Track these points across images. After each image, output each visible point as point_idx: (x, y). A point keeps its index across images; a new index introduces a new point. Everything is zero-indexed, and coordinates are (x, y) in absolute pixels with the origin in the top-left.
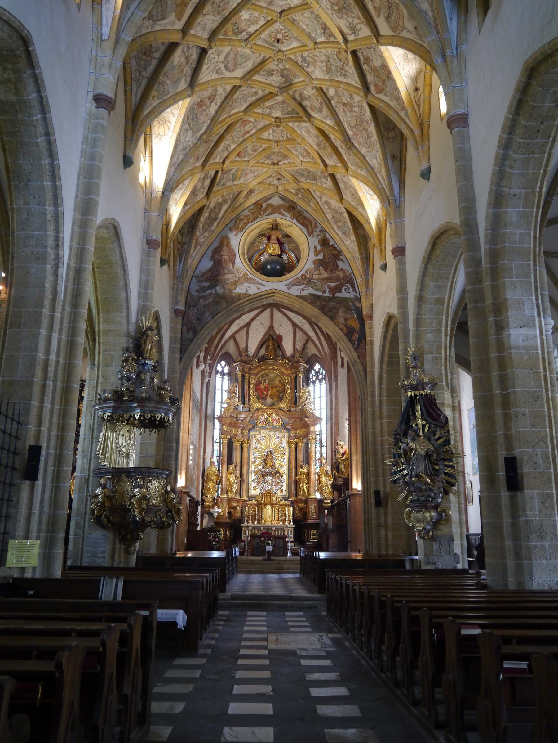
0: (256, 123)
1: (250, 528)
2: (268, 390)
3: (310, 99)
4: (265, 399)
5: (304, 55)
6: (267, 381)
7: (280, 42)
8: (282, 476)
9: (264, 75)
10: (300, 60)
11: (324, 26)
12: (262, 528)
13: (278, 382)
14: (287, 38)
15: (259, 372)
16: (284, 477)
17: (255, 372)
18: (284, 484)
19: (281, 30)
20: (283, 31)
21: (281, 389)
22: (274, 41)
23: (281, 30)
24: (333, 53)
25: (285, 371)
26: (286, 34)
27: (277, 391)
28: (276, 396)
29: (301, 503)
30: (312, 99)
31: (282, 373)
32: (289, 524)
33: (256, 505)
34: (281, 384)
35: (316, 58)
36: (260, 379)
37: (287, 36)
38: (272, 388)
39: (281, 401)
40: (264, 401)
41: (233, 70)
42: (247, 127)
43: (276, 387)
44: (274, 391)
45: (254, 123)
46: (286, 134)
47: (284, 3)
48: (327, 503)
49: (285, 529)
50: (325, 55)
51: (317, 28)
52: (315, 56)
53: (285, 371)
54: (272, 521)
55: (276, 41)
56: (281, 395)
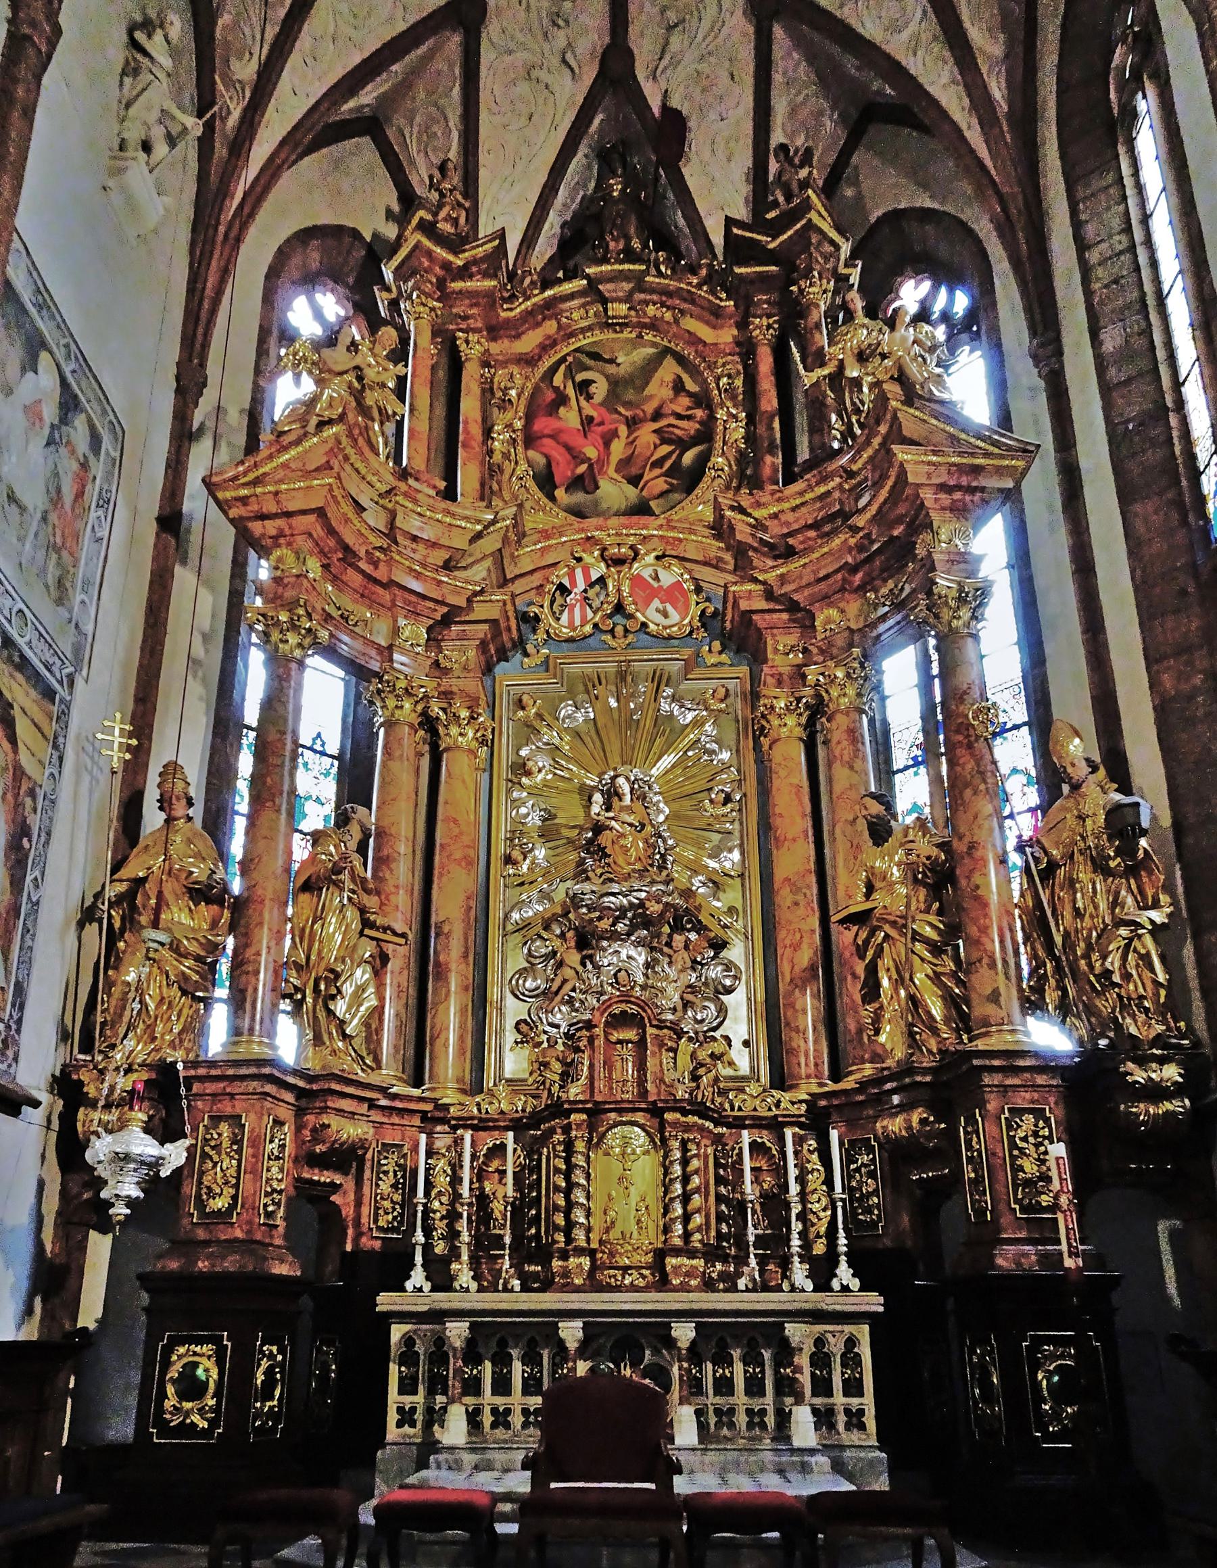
1: (457, 1331)
2: (608, 439)
4: (585, 483)
6: (600, 389)
8: (719, 945)
12: (571, 1332)
13: (667, 393)
15: (547, 346)
16: (736, 953)
17: (529, 342)
18: (737, 1001)
21: (692, 427)
25: (705, 333)
27: (664, 437)
28: (659, 463)
29: (904, 1108)
31: (694, 340)
32: (822, 1284)
33: (517, 1126)
34: (685, 401)
36: (558, 380)
38: (632, 424)
39: (689, 490)
40: (579, 497)
43: (657, 415)
44: (646, 434)
48: (1155, 1092)
49: (795, 1332)
53: (705, 333)
54: (660, 1255)
56: (688, 457)
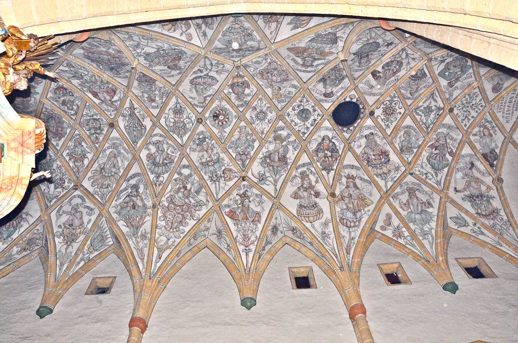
0: (109, 102)
3: (159, 152)
5: (207, 140)
7: (215, 118)
9: (176, 106)
10: (201, 137)
11: (246, 153)
14: (220, 123)
19: (228, 118)
20: (227, 120)
22: (216, 113)
23: (228, 118)
24: (226, 165)
26: (224, 123)
30: (162, 154)
35: (210, 151)
37: (223, 123)
41: (191, 82)
42: (105, 94)
45: (110, 100)
46: (96, 133)
47: (254, 119)
50: (218, 159)
51: (242, 148)
52: (212, 149)
55: (216, 114)
